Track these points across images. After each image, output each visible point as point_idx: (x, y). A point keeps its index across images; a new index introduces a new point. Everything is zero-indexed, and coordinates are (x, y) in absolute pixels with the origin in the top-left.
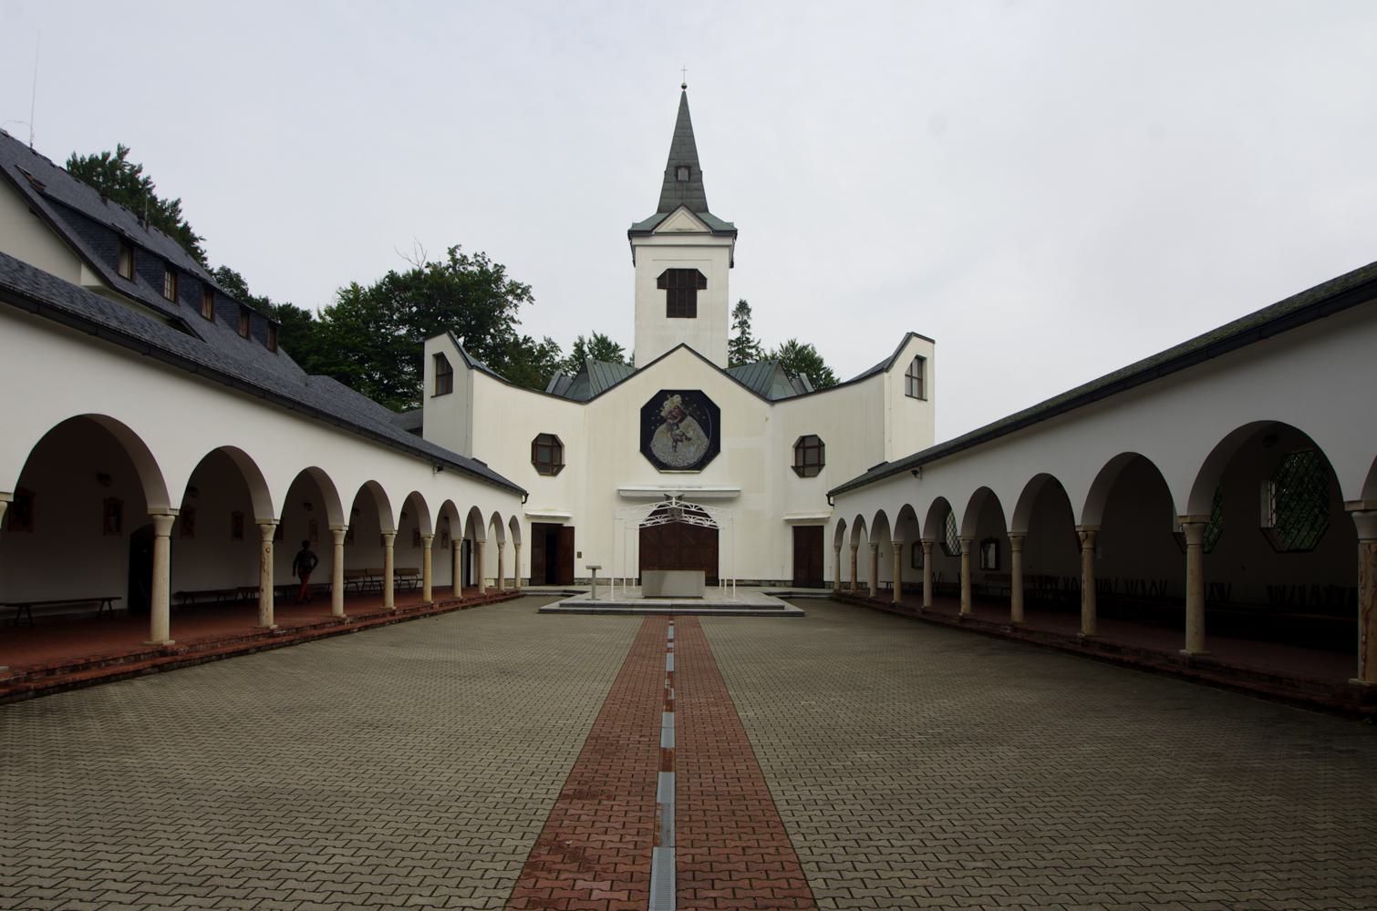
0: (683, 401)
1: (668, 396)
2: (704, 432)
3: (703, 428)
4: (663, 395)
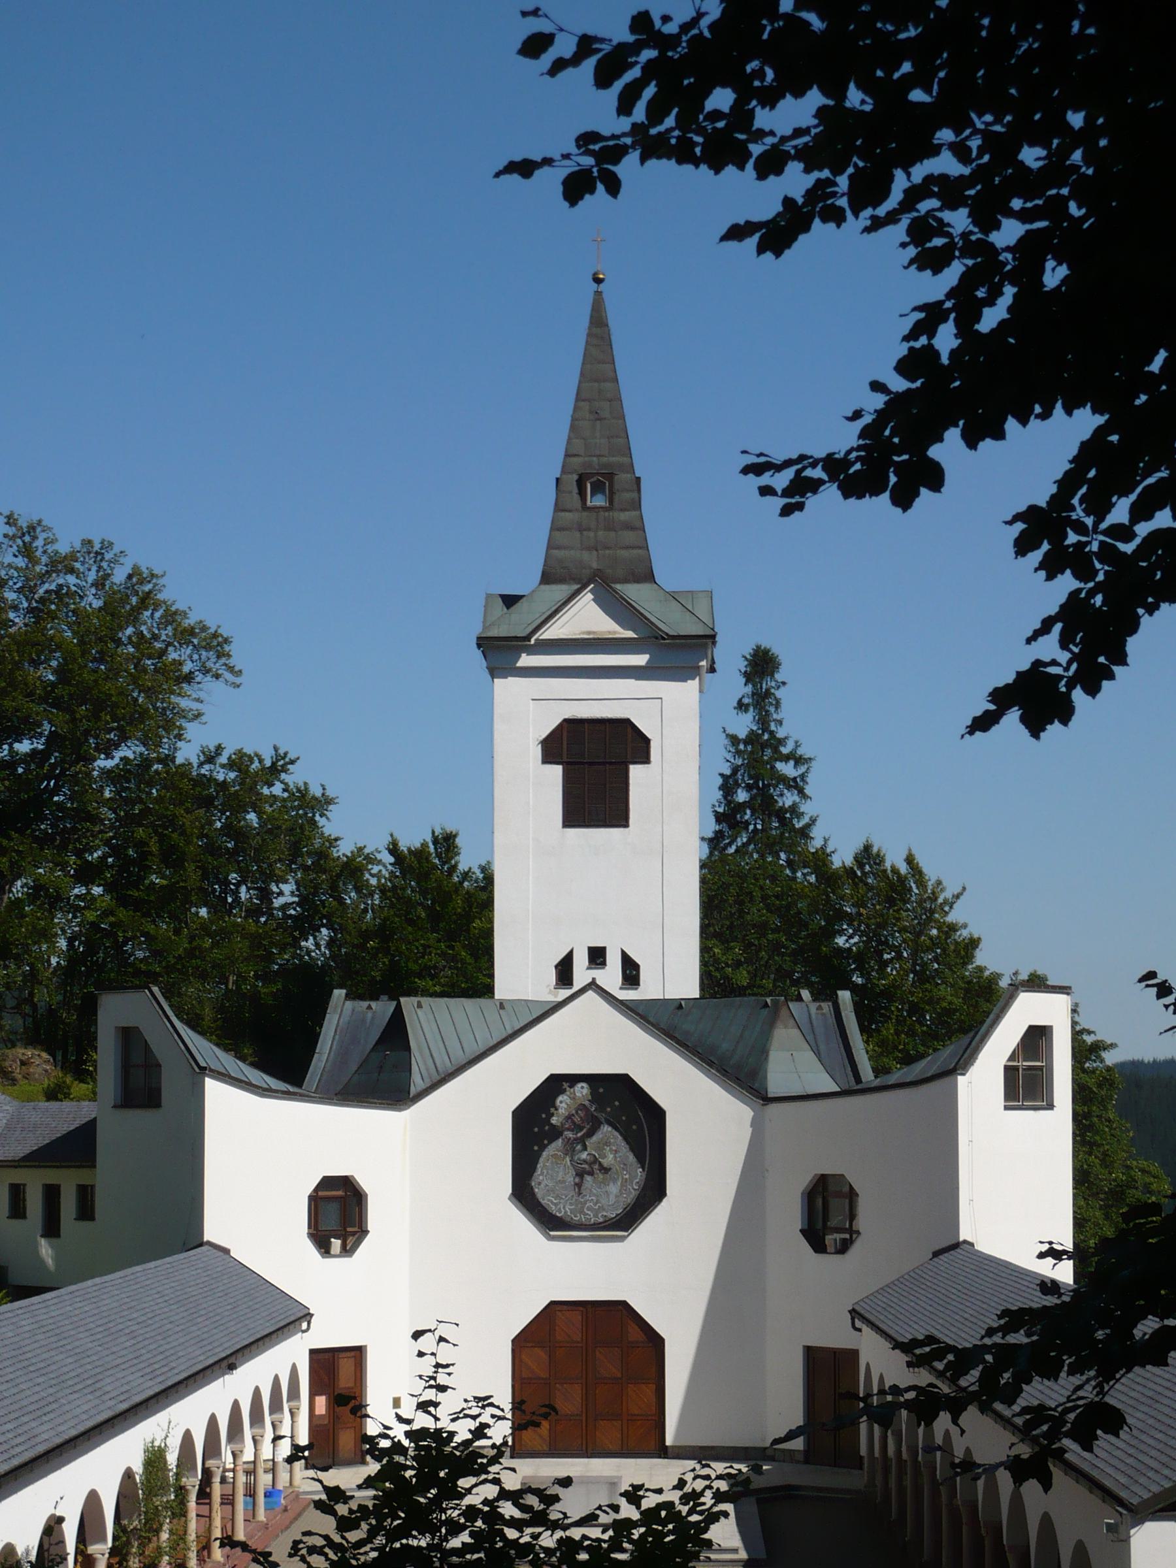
0: (595, 1097)
1: (566, 1085)
2: (636, 1156)
3: (632, 1149)
4: (555, 1084)
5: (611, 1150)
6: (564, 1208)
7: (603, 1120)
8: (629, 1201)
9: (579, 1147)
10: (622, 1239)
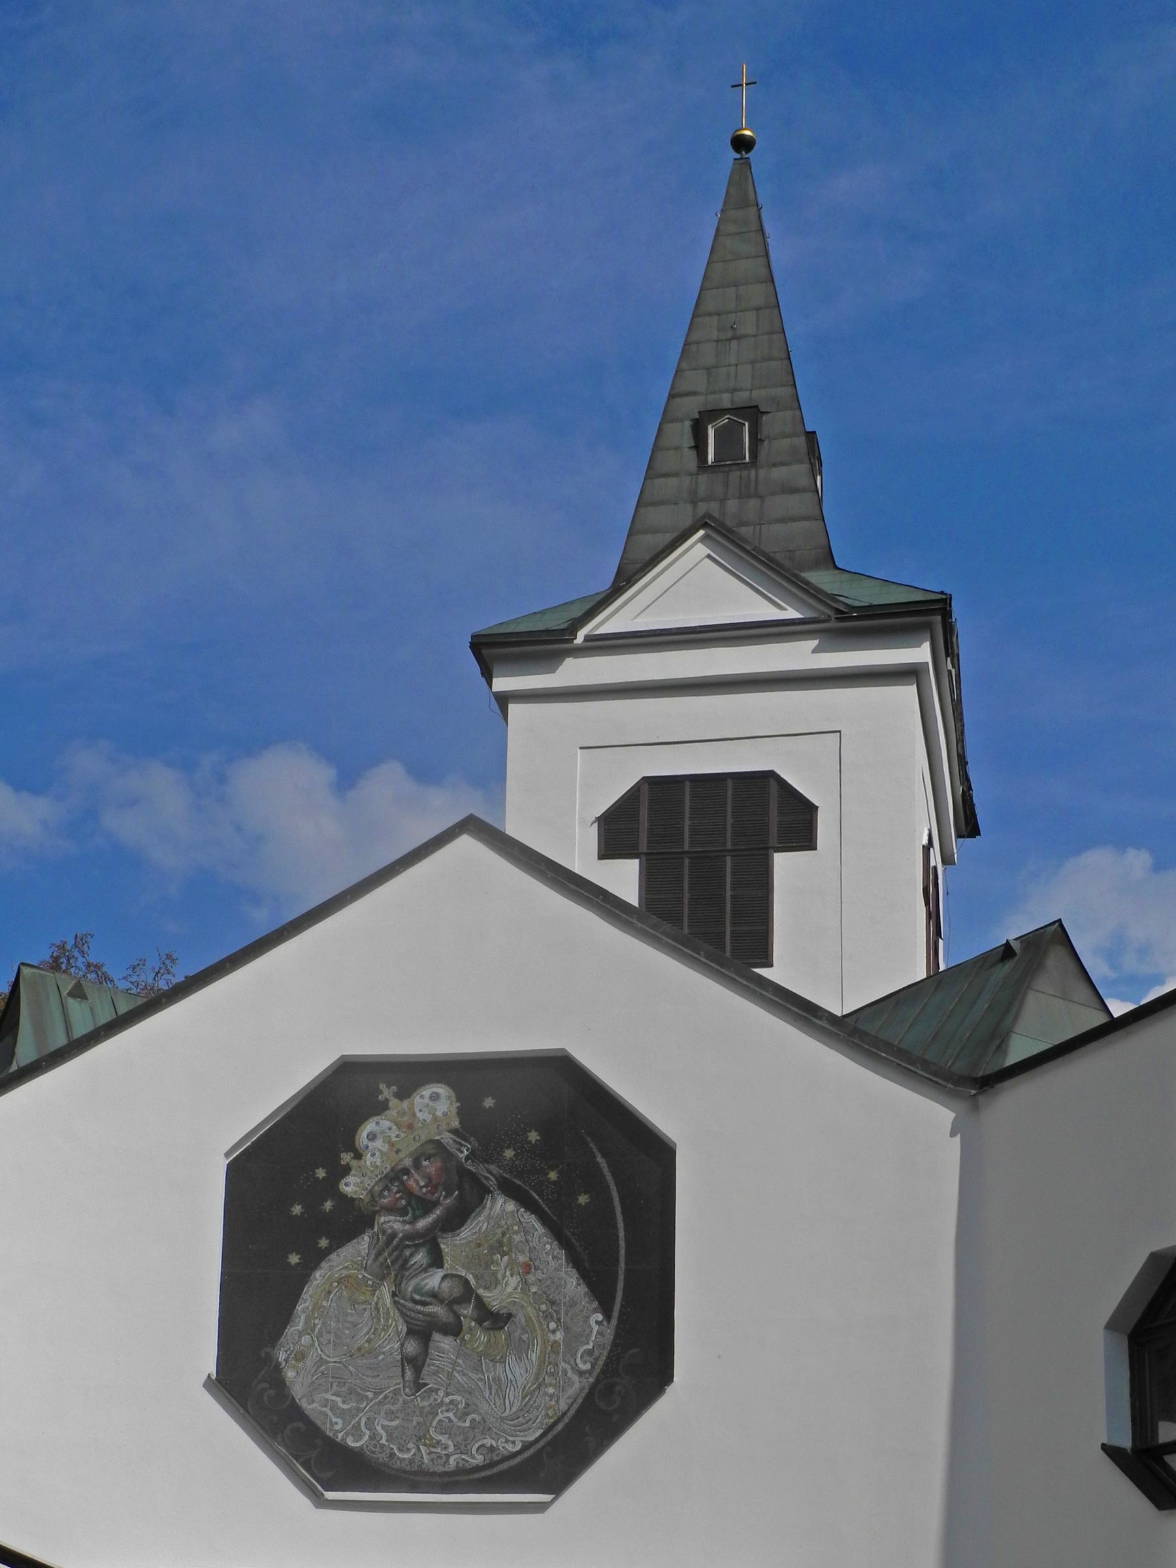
2: (585, 1276)
3: (575, 1261)
5: (511, 1265)
6: (370, 1424)
7: (492, 1183)
8: (563, 1406)
9: (421, 1257)
10: (541, 1507)
